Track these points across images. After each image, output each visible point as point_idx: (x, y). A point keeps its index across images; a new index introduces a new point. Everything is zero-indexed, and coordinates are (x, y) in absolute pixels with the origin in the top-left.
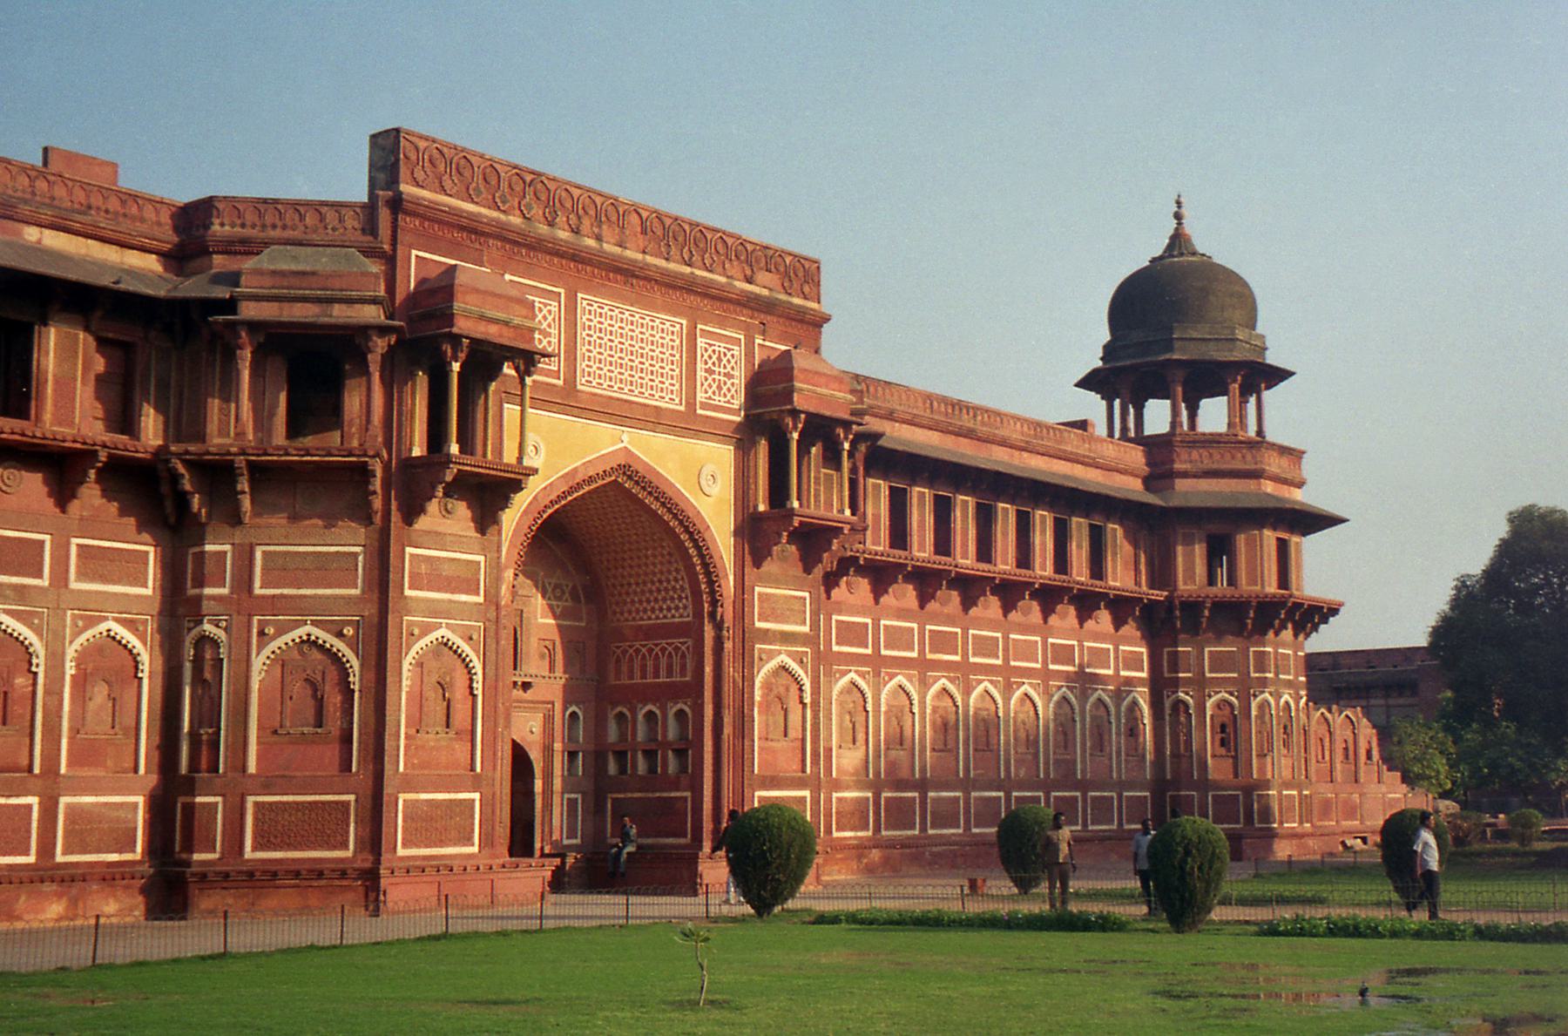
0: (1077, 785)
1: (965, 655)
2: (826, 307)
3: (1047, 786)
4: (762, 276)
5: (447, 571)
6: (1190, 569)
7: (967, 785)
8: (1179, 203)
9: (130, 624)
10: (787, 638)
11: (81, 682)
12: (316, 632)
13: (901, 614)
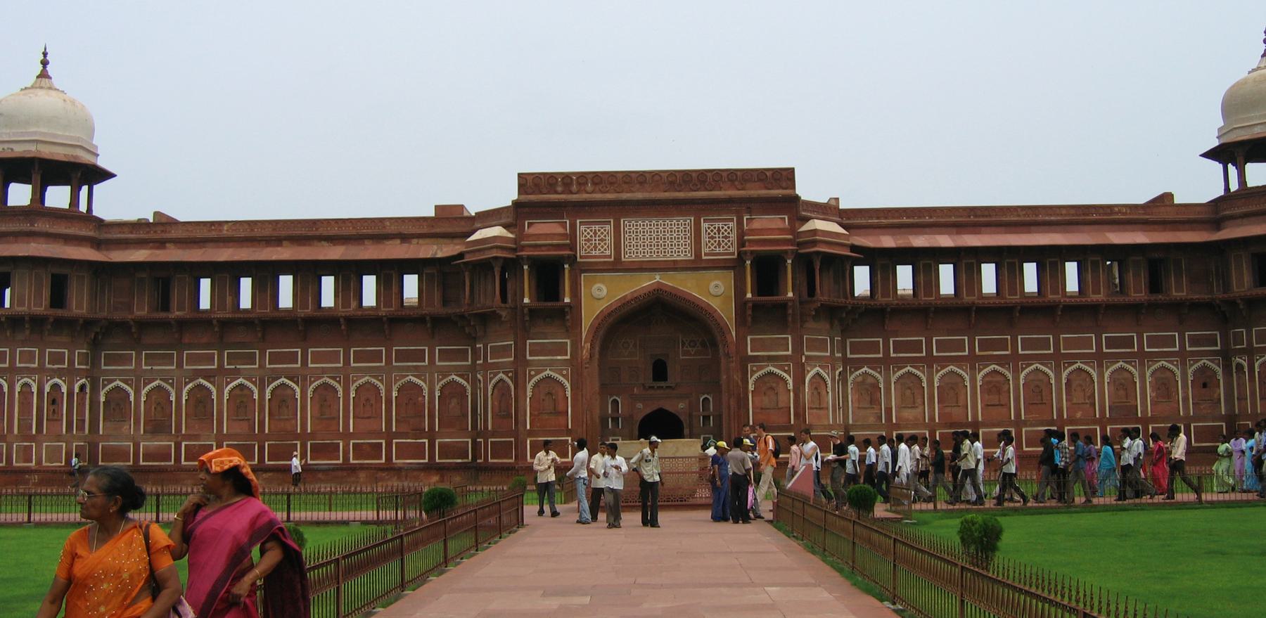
0: (1138, 420)
3: (1103, 422)
4: (748, 185)
10: (770, 359)
12: (504, 377)
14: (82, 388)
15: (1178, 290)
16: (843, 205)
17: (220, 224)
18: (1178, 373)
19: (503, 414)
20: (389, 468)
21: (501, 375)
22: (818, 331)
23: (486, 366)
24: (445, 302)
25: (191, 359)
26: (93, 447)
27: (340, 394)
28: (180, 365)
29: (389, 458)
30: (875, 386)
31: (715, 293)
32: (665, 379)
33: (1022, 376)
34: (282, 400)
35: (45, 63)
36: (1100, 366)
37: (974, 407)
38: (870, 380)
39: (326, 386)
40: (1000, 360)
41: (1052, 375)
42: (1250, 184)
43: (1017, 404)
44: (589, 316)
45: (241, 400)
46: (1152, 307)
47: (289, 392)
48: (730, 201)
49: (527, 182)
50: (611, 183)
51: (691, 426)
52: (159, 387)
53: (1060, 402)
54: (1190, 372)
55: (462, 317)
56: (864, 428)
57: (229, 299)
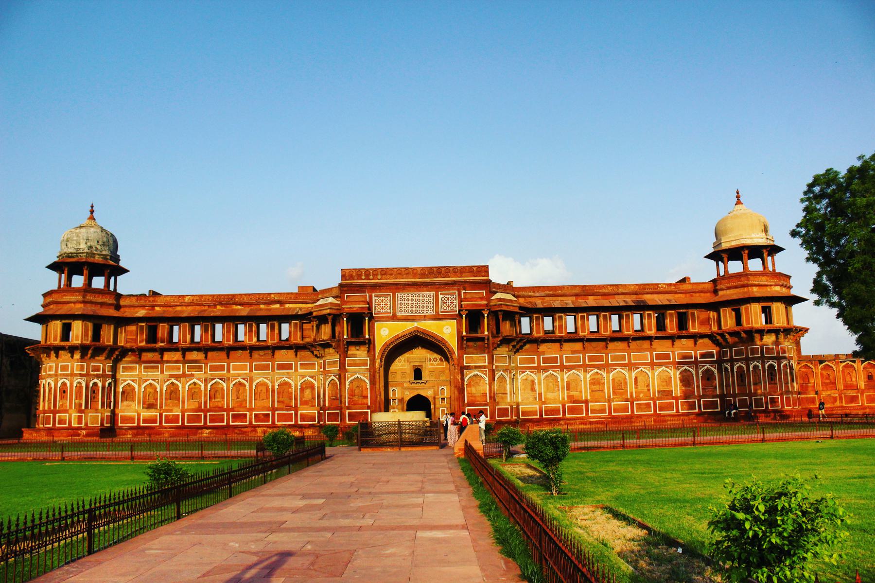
0: (673, 398)
1: (607, 361)
2: (490, 278)
5: (358, 362)
6: (726, 321)
7: (609, 401)
8: (738, 192)
9: (312, 377)
10: (476, 367)
11: (302, 389)
13: (573, 352)
14: (110, 384)
15: (694, 328)
16: (515, 285)
17: (184, 296)
18: (694, 372)
19: (334, 399)
20: (273, 426)
21: (333, 377)
22: (502, 352)
23: (325, 373)
24: (303, 338)
25: (169, 369)
26: (114, 415)
27: (247, 387)
28: (162, 372)
29: (273, 421)
30: (533, 382)
31: (448, 332)
32: (421, 379)
33: (611, 375)
34: (215, 392)
35: (92, 212)
36: (653, 369)
37: (586, 394)
38: (530, 378)
39: (240, 384)
40: (599, 367)
41: (627, 375)
42: (730, 272)
43: (608, 389)
44: (379, 346)
45: (193, 393)
46: (680, 337)
47: (220, 386)
48: (454, 283)
49: (345, 274)
50: (391, 274)
51: (435, 404)
52: (151, 384)
53: (631, 388)
54: (700, 372)
55: (312, 346)
56: (526, 404)
57: (188, 337)
